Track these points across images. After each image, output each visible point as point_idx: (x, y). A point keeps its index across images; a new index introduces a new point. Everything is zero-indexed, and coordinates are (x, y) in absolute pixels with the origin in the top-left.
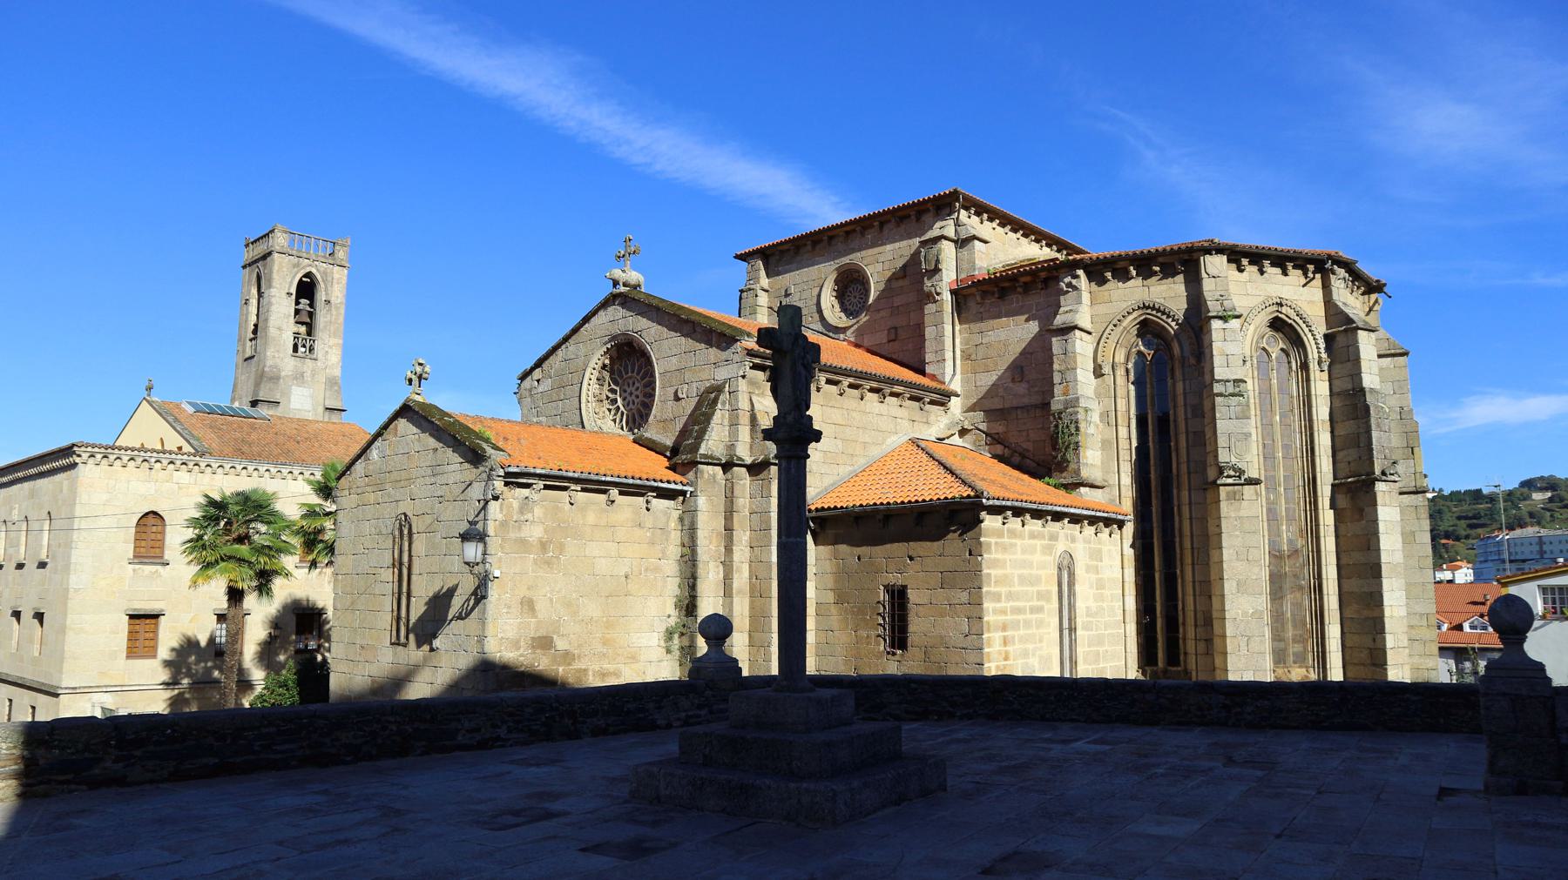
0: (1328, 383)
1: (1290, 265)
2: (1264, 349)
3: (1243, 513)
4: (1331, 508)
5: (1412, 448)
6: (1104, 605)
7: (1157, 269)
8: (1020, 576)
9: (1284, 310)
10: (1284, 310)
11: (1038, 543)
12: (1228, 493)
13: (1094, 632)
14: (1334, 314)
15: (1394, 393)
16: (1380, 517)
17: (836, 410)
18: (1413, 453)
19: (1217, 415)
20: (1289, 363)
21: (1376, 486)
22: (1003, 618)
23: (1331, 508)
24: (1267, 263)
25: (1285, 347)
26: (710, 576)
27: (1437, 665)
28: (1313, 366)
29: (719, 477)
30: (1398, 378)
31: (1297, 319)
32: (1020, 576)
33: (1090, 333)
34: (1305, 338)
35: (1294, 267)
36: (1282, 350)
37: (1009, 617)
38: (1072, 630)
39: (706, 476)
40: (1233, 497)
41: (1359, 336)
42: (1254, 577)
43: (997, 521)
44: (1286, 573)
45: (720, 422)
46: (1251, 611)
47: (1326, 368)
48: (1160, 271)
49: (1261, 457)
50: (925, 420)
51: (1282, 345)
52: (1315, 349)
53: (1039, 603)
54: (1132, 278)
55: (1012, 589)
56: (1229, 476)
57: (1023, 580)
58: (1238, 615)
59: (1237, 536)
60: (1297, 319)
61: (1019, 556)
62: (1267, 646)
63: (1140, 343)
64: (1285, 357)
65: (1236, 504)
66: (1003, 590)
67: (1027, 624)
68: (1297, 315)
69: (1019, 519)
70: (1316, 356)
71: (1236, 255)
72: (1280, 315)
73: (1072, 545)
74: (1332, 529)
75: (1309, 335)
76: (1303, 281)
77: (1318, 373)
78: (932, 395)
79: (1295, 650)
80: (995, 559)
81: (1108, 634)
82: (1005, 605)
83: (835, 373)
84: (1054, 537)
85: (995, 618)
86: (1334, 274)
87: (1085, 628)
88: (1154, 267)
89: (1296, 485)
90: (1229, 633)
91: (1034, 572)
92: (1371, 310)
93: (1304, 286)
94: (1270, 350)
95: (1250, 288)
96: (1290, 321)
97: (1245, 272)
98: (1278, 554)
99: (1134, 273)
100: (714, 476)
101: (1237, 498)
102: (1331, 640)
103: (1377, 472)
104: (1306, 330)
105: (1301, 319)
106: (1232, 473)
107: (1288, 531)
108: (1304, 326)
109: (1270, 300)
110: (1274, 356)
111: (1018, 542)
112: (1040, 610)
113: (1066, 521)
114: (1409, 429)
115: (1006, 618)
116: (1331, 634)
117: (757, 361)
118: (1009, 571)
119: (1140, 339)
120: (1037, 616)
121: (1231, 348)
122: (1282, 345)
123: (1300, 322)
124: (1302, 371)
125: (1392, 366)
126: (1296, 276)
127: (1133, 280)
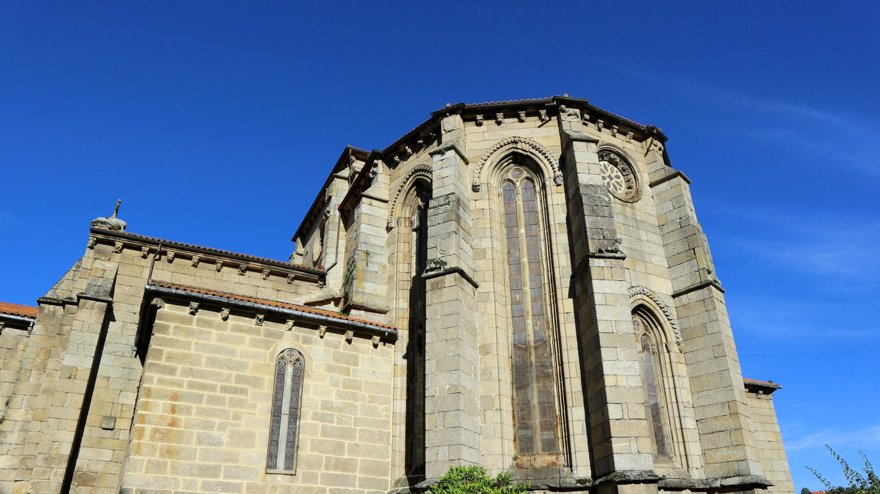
0: (564, 194)
1: (522, 114)
2: (509, 180)
3: (444, 299)
4: (570, 297)
5: (693, 249)
6: (358, 404)
7: (421, 141)
8: (208, 358)
9: (519, 145)
10: (519, 145)
11: (248, 337)
12: (432, 284)
13: (335, 425)
14: (567, 142)
15: (674, 208)
16: (595, 290)
17: (187, 276)
18: (695, 254)
19: (429, 223)
20: (534, 187)
21: (590, 262)
22: (176, 389)
23: (570, 297)
24: (500, 116)
25: (529, 176)
26: (31, 379)
27: (745, 455)
28: (549, 183)
29: (59, 313)
30: (675, 196)
31: (533, 151)
32: (208, 358)
33: (386, 202)
34: (541, 164)
35: (527, 115)
36: (527, 178)
37: (185, 390)
38: (294, 416)
39: (46, 311)
40: (435, 287)
41: (574, 146)
42: (451, 355)
43: (185, 311)
44: (531, 363)
45: (71, 278)
46: (447, 387)
47: (560, 181)
48: (424, 143)
49: (507, 267)
50: (293, 291)
51: (525, 174)
52: (551, 170)
53: (239, 386)
54: (411, 155)
55: (195, 367)
56: (432, 270)
57: (211, 362)
58: (436, 392)
59: (438, 320)
60: (533, 151)
61: (213, 342)
62: (509, 432)
63: (420, 200)
64: (530, 183)
65: (439, 291)
66: (180, 367)
67: (212, 400)
68: (533, 148)
69: (220, 314)
70: (552, 175)
71: (469, 115)
72: (515, 150)
73: (305, 346)
74: (572, 315)
75: (546, 161)
76: (540, 123)
77: (554, 188)
78: (295, 271)
79: (545, 437)
80: (171, 339)
81: (360, 430)
82: (181, 378)
83: (183, 249)
84: (280, 336)
85: (158, 387)
86: (564, 111)
87: (315, 417)
88: (419, 142)
89: (543, 284)
90: (428, 410)
91: (237, 358)
92: (648, 151)
93: (539, 127)
94: (514, 180)
95: (487, 135)
96: (525, 153)
97: (482, 127)
98: (524, 346)
99: (409, 150)
100: (54, 313)
101: (439, 287)
102: (575, 423)
103: (592, 249)
104: (542, 157)
105: (536, 150)
106: (433, 265)
107: (535, 325)
108: (540, 155)
109: (504, 141)
110: (518, 184)
111: (214, 332)
112: (243, 392)
113: (291, 323)
114: (688, 234)
115: (181, 389)
116: (574, 417)
117: (100, 236)
118: (192, 351)
119: (419, 198)
120: (232, 395)
121: (446, 172)
122: (525, 174)
123: (537, 153)
124: (543, 191)
125: (669, 188)
126: (533, 121)
127: (411, 157)
